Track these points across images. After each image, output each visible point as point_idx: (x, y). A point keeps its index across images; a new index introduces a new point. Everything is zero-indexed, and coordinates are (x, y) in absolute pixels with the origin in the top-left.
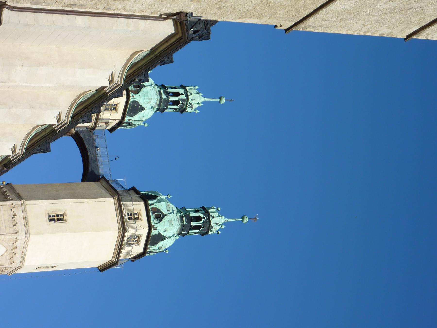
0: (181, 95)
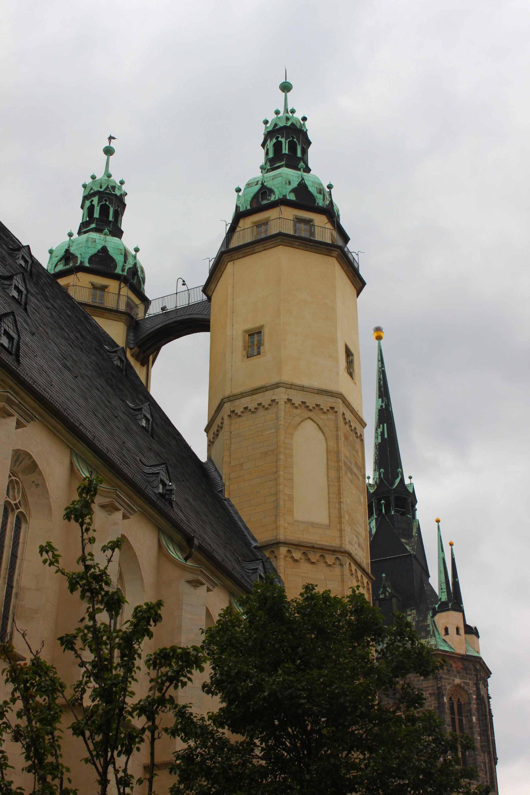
0: (93, 203)
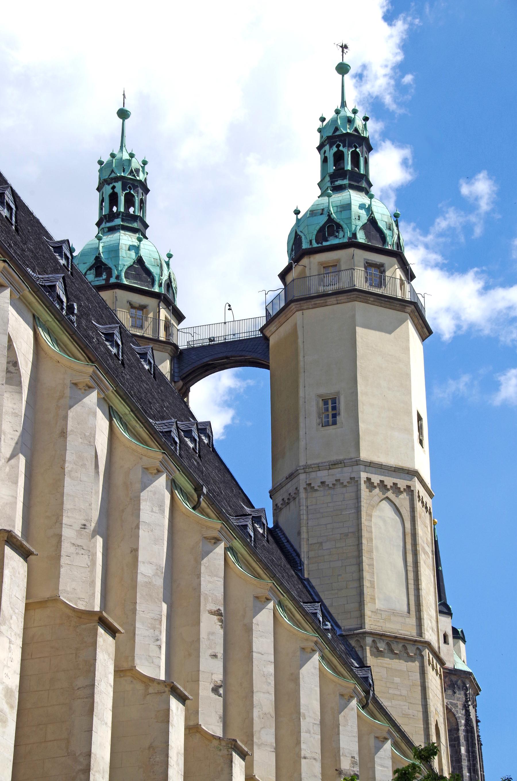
0: (116, 190)
